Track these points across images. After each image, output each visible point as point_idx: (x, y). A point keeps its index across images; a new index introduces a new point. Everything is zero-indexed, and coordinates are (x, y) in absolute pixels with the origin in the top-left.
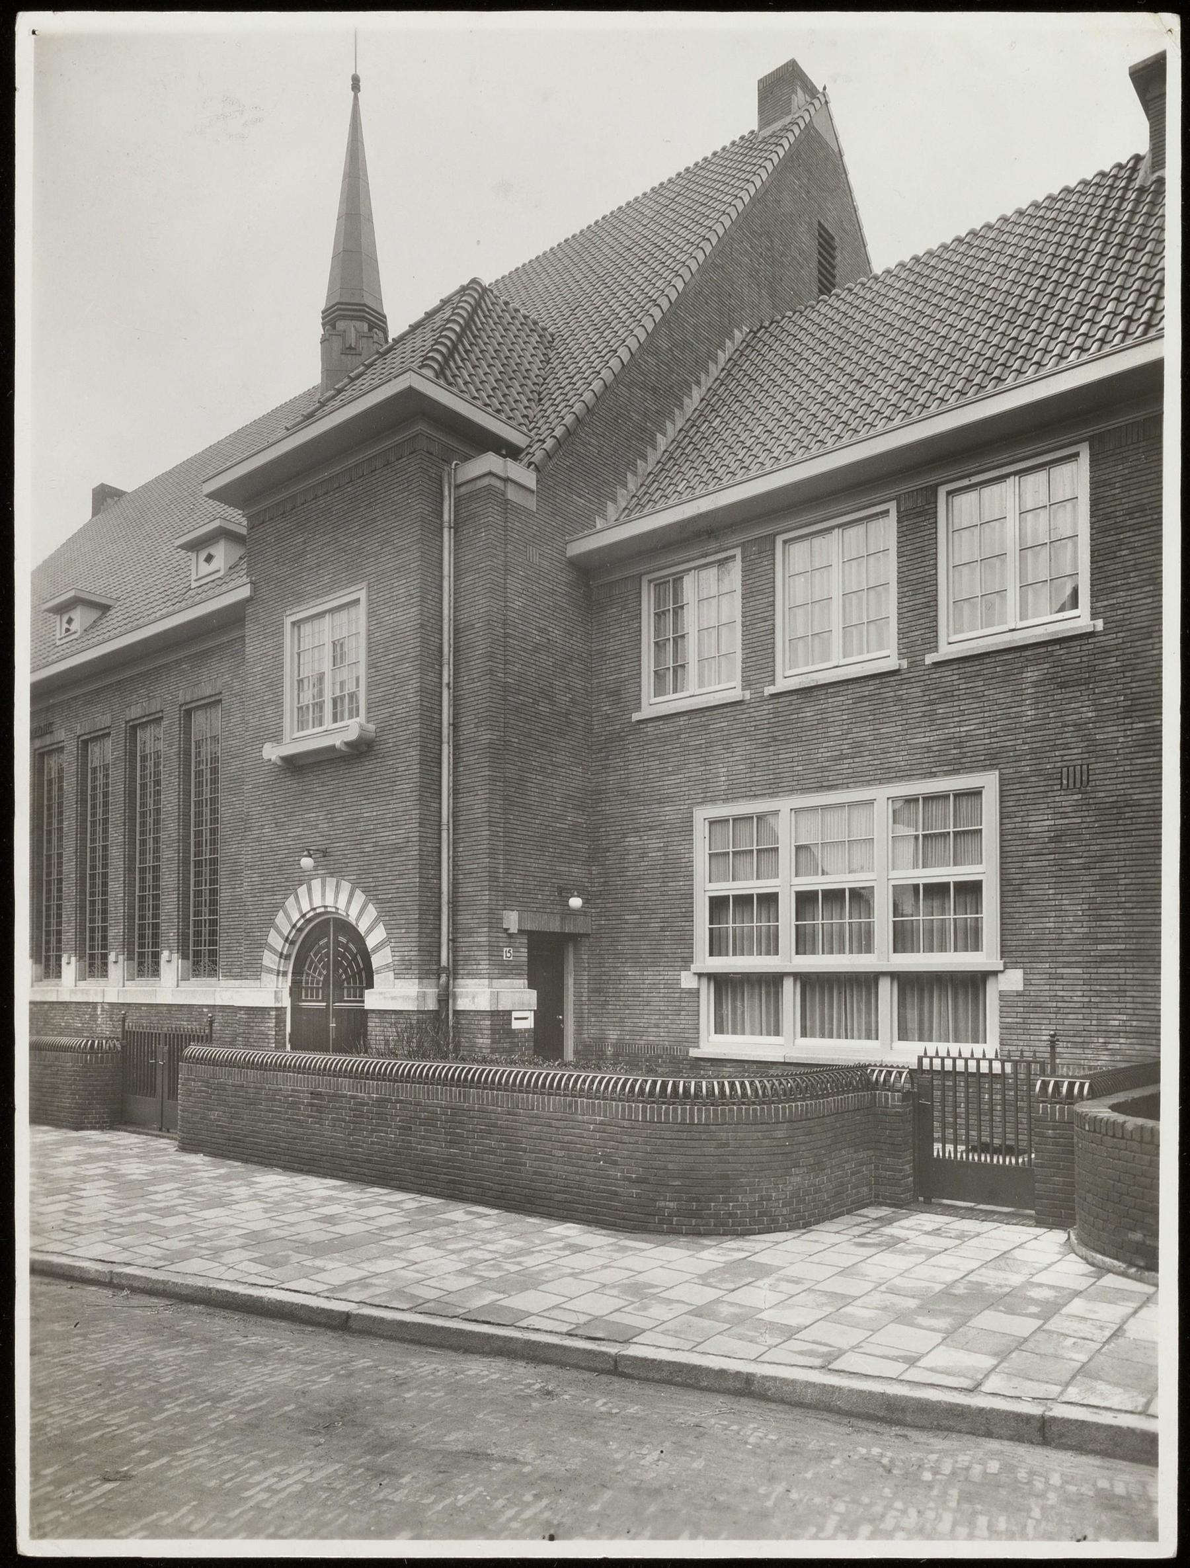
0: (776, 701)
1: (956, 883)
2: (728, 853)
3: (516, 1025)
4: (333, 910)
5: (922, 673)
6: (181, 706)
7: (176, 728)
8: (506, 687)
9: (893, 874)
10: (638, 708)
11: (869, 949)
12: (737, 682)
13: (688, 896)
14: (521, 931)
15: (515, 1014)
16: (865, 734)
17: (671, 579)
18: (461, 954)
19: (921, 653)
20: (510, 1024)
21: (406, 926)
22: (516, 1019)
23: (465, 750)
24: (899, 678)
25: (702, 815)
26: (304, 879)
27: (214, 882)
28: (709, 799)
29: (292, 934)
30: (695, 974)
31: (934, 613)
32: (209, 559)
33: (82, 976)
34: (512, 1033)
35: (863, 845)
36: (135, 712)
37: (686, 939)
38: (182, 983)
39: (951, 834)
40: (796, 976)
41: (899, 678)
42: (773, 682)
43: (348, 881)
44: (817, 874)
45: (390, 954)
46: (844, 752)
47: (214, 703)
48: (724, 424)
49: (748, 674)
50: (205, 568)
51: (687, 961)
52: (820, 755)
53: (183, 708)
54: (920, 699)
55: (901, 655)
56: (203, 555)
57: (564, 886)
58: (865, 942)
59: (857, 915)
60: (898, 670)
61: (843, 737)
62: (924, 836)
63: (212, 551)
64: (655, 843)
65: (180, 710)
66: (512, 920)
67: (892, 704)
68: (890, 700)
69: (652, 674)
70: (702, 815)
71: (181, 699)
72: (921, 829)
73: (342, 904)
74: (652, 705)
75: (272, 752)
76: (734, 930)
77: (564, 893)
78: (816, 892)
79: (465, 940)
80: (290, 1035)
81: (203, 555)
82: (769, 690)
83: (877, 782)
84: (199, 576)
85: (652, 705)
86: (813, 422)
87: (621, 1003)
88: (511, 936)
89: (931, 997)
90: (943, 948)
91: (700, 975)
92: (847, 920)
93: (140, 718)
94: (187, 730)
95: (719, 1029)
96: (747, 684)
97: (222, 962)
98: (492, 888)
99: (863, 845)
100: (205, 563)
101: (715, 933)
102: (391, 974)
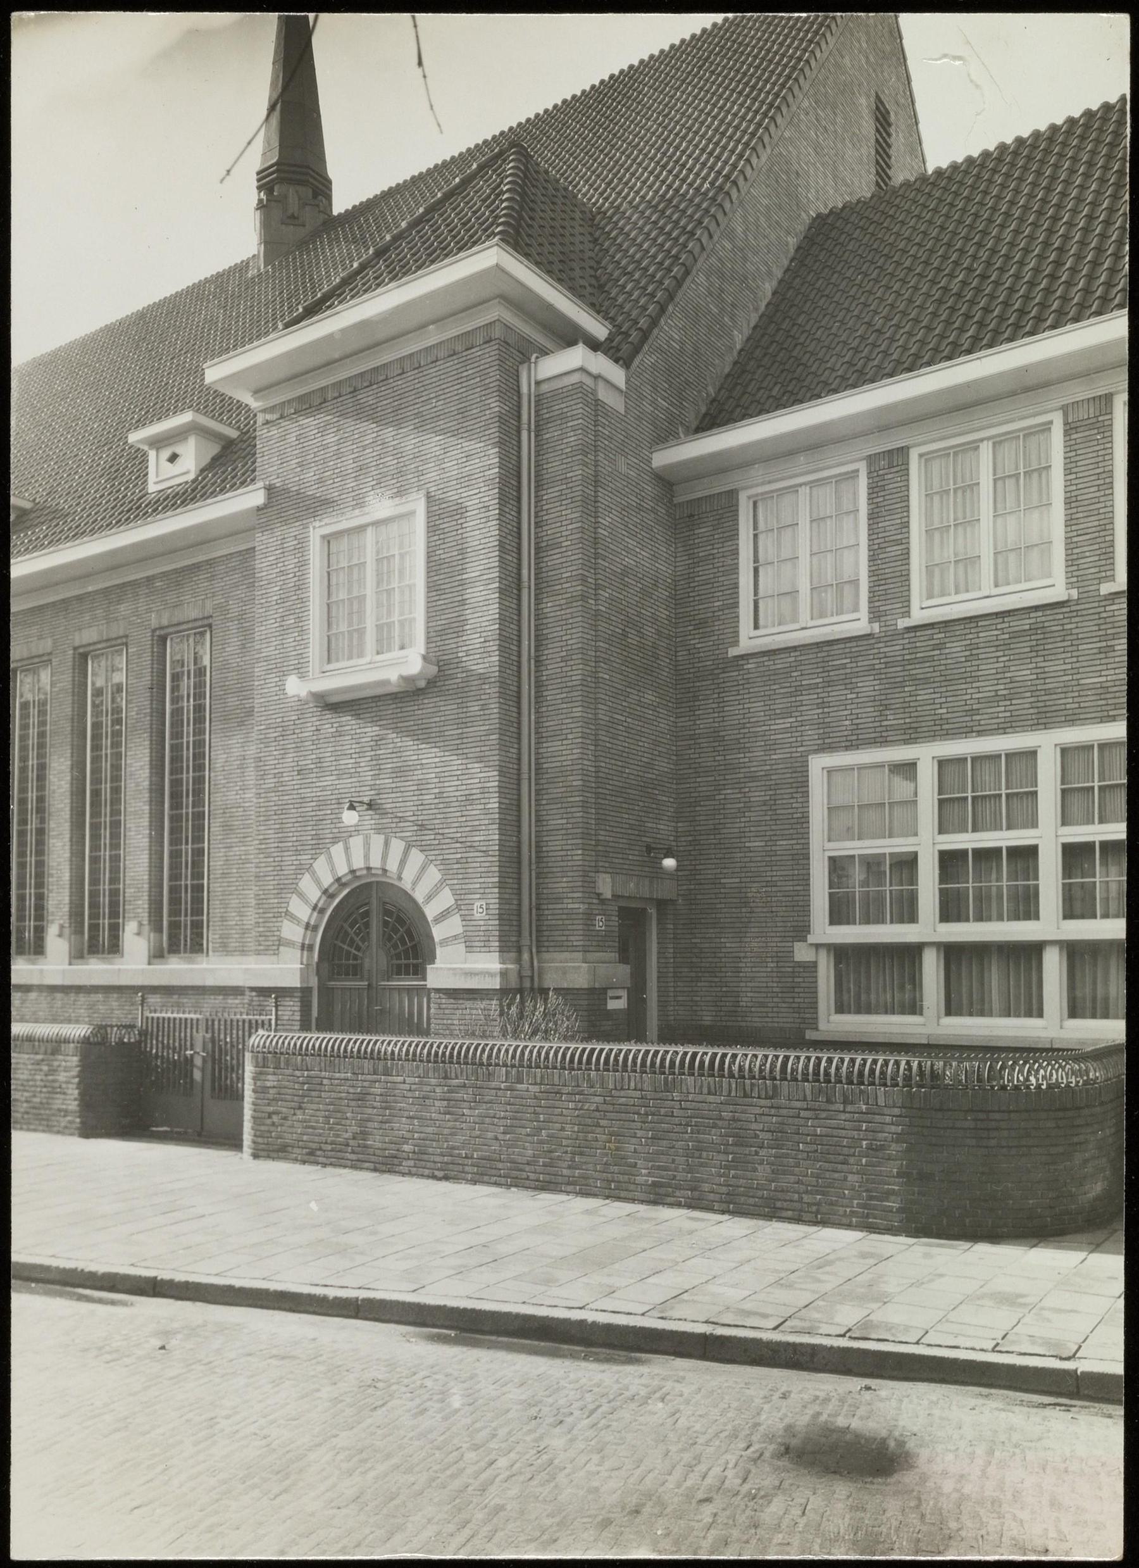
0: (913, 634)
1: (974, 850)
2: (1000, 796)
3: (612, 1005)
4: (380, 872)
5: (1096, 604)
6: (154, 631)
7: (147, 657)
8: (597, 614)
9: (832, 845)
10: (736, 643)
11: (912, 918)
12: (864, 612)
13: (802, 857)
14: (616, 897)
15: (610, 993)
16: (1025, 673)
17: (952, 451)
18: (546, 923)
19: (1095, 582)
20: (606, 1004)
21: (482, 891)
22: (612, 998)
23: (550, 687)
24: (1068, 610)
25: (818, 764)
26: (342, 836)
27: (198, 839)
28: (826, 747)
29: (322, 902)
30: (811, 945)
31: (1110, 538)
32: (173, 458)
33: (78, 955)
34: (610, 1015)
35: (956, 805)
36: (88, 636)
37: (803, 907)
38: (73, 961)
39: (970, 799)
40: (938, 945)
41: (1068, 610)
42: (907, 614)
43: (402, 838)
44: (1093, 823)
45: (460, 923)
46: (1000, 693)
47: (204, 626)
48: (812, 322)
49: (877, 604)
50: (169, 469)
51: (802, 931)
52: (968, 697)
53: (158, 633)
54: (1094, 634)
55: (1070, 585)
56: (166, 454)
57: (654, 846)
58: (908, 911)
59: (1079, 873)
60: (1068, 601)
61: (999, 676)
62: (1008, 795)
63: (178, 449)
64: (757, 796)
65: (153, 636)
66: (605, 886)
67: (1059, 639)
68: (1057, 634)
69: (924, 569)
70: (818, 764)
71: (154, 623)
72: (1003, 787)
73: (392, 866)
74: (748, 639)
75: (295, 687)
76: (891, 891)
77: (653, 852)
78: (965, 852)
79: (550, 906)
80: (317, 1019)
81: (166, 454)
82: (902, 623)
83: (1042, 727)
84: (160, 479)
85: (748, 639)
86: (845, 350)
87: (717, 980)
88: (603, 901)
89: (868, 968)
90: (880, 920)
91: (818, 946)
92: (888, 888)
93: (95, 643)
94: (160, 659)
95: (840, 1009)
96: (875, 615)
97: (211, 936)
98: (587, 847)
99: (956, 805)
100: (169, 464)
101: (1078, 893)
102: (462, 947)
